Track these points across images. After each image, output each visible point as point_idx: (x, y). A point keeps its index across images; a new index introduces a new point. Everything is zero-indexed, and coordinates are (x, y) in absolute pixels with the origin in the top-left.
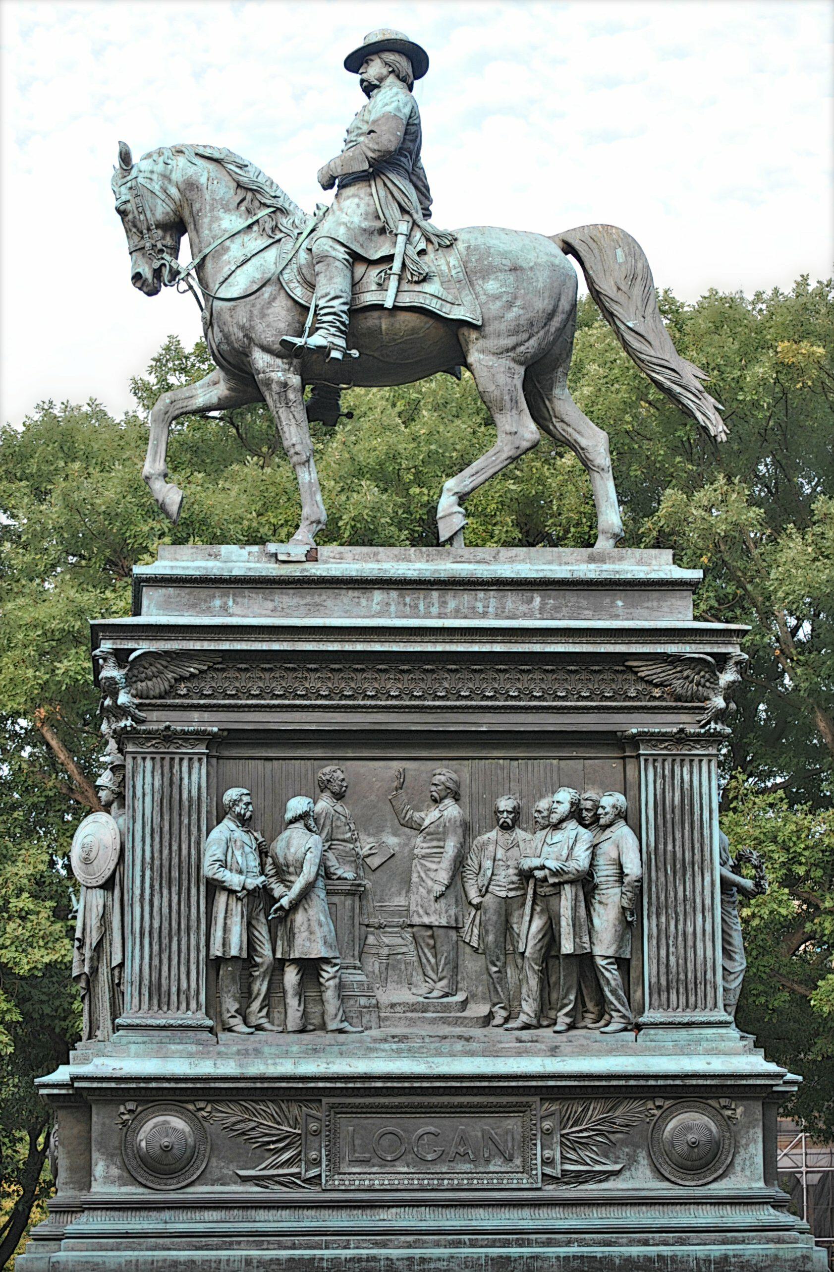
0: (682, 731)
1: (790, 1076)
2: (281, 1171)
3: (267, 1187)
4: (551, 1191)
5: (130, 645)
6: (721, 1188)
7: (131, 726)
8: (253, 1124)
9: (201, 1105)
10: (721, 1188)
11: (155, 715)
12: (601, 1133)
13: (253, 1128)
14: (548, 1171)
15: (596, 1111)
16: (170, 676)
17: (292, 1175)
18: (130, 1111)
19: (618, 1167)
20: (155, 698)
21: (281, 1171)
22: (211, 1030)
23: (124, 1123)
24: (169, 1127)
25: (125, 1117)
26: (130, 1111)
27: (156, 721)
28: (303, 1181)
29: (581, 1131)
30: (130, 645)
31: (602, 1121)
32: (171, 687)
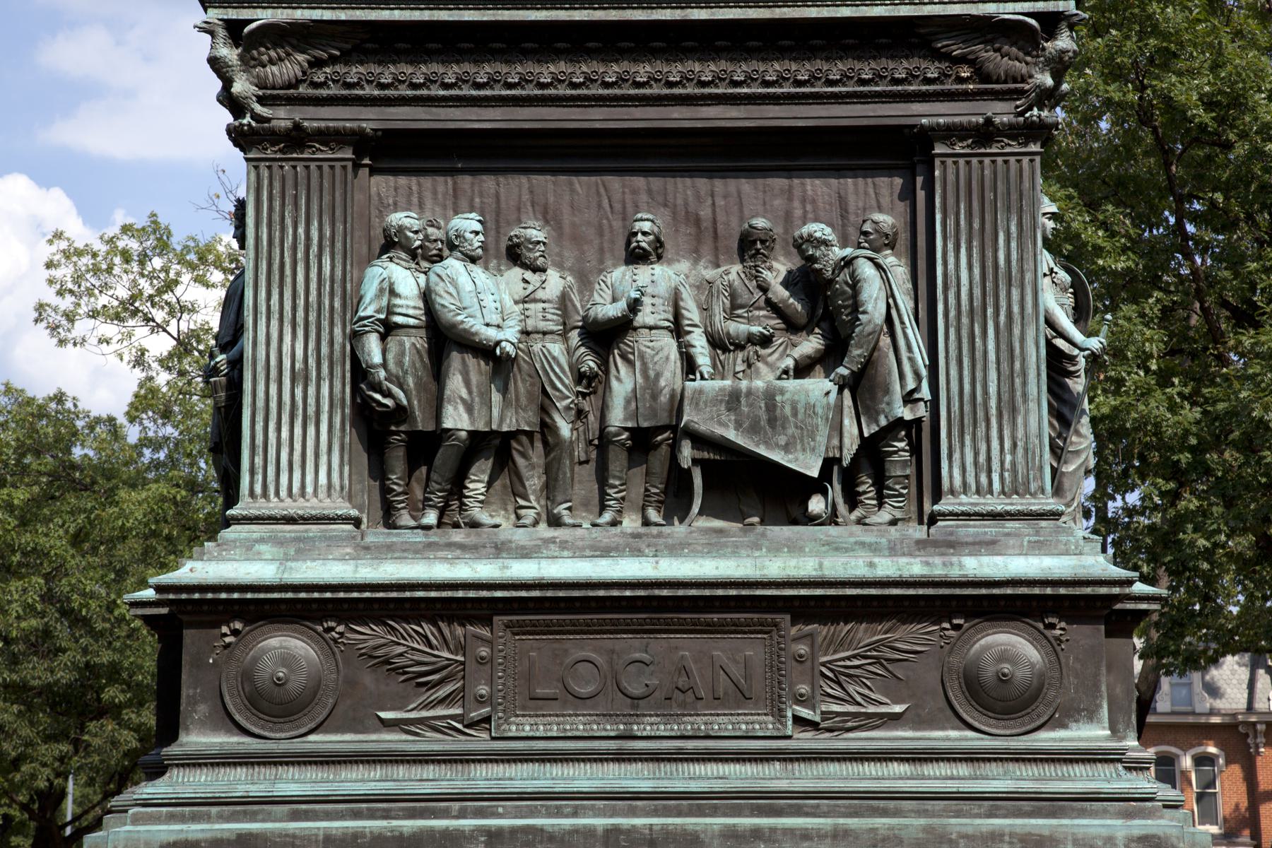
0: (989, 121)
1: (1139, 588)
2: (440, 711)
3: (417, 734)
4: (805, 740)
5: (244, 14)
6: (1047, 738)
7: (249, 125)
8: (401, 649)
9: (332, 624)
10: (1047, 738)
11: (282, 112)
12: (878, 661)
13: (401, 655)
14: (805, 713)
15: (866, 634)
16: (301, 57)
17: (453, 717)
18: (235, 633)
19: (898, 709)
20: (281, 88)
21: (440, 711)
22: (357, 522)
23: (227, 646)
24: (287, 650)
25: (228, 640)
26: (235, 633)
27: (282, 117)
28: (465, 726)
29: (848, 658)
30: (244, 14)
31: (875, 646)
32: (304, 73)
